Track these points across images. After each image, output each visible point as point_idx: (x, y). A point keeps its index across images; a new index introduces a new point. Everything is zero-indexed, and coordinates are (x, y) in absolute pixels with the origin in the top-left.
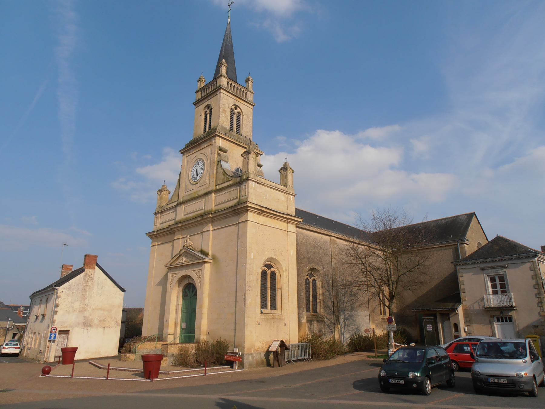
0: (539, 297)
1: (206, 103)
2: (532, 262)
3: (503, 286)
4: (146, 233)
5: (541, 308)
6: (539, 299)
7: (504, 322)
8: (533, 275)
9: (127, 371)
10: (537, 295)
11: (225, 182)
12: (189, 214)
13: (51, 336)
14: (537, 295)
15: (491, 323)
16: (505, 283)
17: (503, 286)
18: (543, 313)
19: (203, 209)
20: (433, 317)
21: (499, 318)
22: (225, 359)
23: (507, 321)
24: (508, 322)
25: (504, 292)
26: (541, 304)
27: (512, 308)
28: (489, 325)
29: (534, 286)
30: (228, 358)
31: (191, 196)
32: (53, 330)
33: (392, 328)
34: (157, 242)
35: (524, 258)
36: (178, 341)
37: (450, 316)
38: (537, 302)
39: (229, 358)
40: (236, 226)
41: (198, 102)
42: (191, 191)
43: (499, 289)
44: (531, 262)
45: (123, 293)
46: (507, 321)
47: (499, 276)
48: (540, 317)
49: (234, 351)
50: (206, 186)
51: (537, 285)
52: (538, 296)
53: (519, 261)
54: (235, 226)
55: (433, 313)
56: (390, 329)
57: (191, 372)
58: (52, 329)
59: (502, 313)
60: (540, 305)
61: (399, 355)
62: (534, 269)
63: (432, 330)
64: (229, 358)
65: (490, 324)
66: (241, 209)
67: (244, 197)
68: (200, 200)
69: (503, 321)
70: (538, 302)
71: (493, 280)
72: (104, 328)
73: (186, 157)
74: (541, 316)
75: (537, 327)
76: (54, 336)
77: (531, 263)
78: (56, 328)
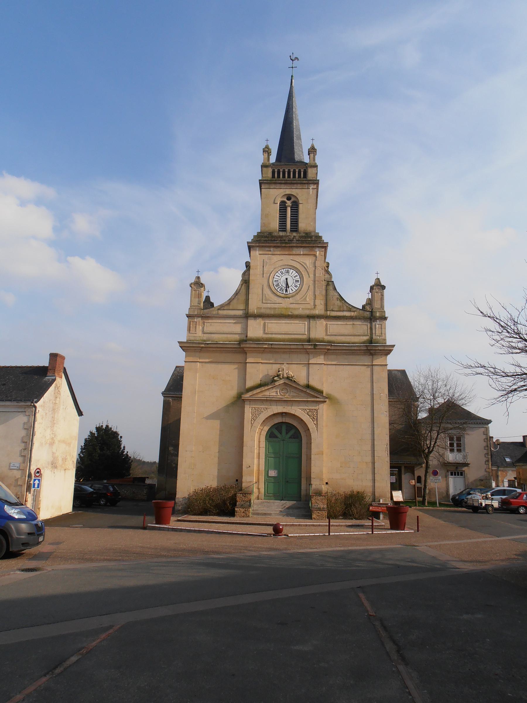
0: (487, 456)
1: (288, 192)
2: (486, 427)
3: (459, 445)
4: (178, 342)
5: (488, 466)
6: (487, 458)
7: (457, 476)
8: (485, 439)
9: (319, 526)
10: (486, 455)
11: (343, 311)
12: (275, 334)
13: (35, 483)
14: (486, 455)
15: (446, 476)
16: (461, 443)
17: (459, 445)
18: (488, 469)
19: (306, 334)
20: (397, 470)
21: (453, 472)
22: (370, 510)
23: (459, 475)
24: (460, 476)
25: (459, 451)
26: (488, 463)
27: (466, 465)
28: (445, 478)
29: (485, 447)
30: (375, 509)
31: (277, 312)
32: (37, 473)
33: (437, 480)
34: (199, 359)
35: (473, 424)
36: (519, 490)
37: (415, 469)
38: (485, 461)
39: (377, 509)
40: (366, 368)
41: (270, 183)
42: (276, 304)
43: (455, 447)
44: (485, 427)
45: (78, 418)
46: (459, 475)
47: (457, 436)
48: (486, 473)
49: (380, 502)
50: (309, 306)
51: (487, 447)
52: (487, 456)
53: (476, 426)
54: (366, 367)
55: (399, 465)
56: (434, 480)
57: (170, 529)
58: (36, 472)
59: (457, 468)
60: (487, 463)
61: (485, 503)
62: (486, 434)
63: (395, 481)
64: (377, 509)
65: (446, 478)
66: (380, 351)
67: (378, 337)
68: (298, 322)
69: (456, 475)
70: (486, 461)
71: (451, 439)
72: (65, 470)
73: (260, 254)
74: (486, 472)
75: (483, 481)
76: (38, 482)
77: (485, 428)
78: (38, 469)
